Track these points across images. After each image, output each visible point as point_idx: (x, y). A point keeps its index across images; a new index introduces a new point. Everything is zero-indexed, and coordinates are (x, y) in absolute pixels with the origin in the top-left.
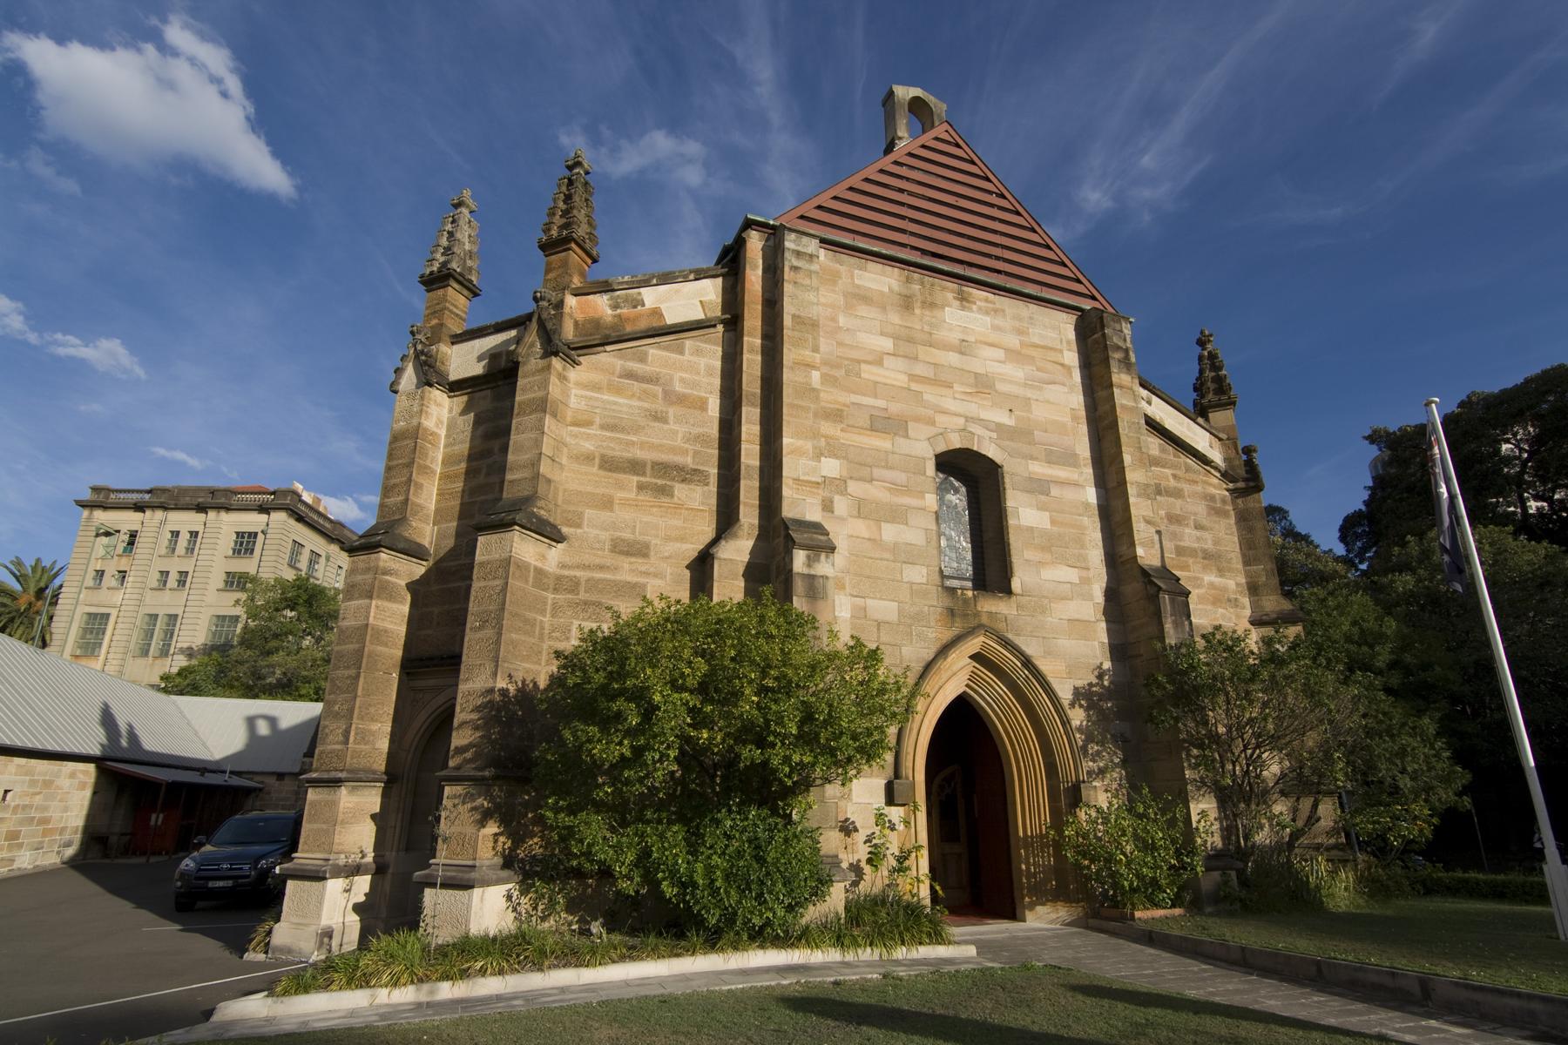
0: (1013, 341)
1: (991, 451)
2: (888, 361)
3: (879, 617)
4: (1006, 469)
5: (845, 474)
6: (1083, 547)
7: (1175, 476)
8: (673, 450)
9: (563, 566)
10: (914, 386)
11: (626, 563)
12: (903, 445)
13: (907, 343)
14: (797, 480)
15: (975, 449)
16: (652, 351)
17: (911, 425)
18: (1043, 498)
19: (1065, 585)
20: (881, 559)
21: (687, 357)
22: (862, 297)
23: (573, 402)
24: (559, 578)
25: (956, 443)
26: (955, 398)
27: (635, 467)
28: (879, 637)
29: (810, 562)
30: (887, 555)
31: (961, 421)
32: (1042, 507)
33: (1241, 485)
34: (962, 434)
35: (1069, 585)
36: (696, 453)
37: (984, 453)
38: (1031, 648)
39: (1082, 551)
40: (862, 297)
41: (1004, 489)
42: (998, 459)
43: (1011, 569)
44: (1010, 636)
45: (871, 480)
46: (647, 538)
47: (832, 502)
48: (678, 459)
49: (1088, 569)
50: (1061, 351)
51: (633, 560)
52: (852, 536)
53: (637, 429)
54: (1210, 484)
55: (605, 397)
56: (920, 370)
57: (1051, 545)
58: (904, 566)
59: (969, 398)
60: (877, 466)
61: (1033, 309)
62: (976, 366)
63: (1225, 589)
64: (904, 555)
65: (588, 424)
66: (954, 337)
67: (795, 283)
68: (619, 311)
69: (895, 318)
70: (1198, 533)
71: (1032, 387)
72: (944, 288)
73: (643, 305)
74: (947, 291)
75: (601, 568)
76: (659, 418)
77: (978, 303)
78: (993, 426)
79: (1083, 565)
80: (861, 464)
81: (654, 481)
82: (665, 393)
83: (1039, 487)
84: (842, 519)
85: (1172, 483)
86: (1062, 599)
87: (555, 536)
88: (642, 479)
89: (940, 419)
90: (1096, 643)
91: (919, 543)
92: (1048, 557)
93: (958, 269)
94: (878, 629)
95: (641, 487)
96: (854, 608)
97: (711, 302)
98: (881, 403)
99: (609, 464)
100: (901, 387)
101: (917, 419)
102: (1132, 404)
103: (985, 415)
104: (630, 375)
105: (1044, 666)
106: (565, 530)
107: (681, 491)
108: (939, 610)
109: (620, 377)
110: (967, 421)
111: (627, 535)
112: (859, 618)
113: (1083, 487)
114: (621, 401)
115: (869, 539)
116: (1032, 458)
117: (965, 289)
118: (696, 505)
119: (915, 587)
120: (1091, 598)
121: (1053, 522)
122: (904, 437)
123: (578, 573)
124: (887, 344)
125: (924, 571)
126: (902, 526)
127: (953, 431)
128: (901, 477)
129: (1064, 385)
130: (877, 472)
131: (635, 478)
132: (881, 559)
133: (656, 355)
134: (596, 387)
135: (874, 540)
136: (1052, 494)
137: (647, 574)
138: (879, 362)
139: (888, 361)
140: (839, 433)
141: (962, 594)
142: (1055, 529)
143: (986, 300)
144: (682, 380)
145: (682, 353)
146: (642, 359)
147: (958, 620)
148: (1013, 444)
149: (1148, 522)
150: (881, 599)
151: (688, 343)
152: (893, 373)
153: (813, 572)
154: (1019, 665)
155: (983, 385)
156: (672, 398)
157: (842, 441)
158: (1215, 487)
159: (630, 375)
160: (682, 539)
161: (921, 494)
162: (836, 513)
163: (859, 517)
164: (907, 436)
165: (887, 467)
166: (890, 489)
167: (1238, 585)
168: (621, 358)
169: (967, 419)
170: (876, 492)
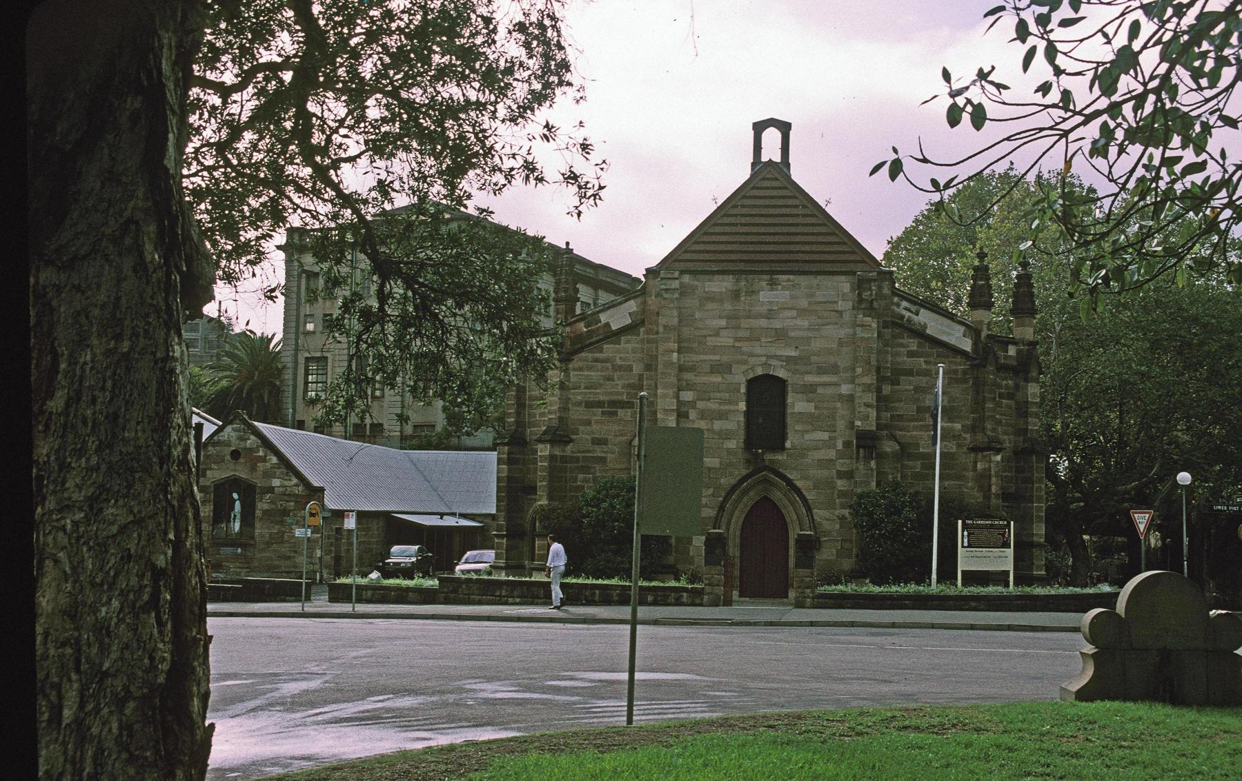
0: (804, 303)
1: (781, 374)
3: (709, 465)
4: (790, 382)
6: (834, 420)
8: (618, 394)
10: (737, 344)
11: (597, 448)
12: (729, 378)
13: (733, 317)
14: (665, 410)
16: (605, 346)
21: (622, 345)
23: (573, 379)
24: (572, 457)
25: (760, 371)
27: (600, 404)
31: (764, 359)
32: (808, 401)
36: (628, 393)
40: (710, 298)
42: (785, 378)
45: (709, 400)
48: (620, 398)
50: (837, 302)
53: (601, 385)
56: (741, 334)
57: (812, 421)
62: (777, 324)
63: (952, 429)
64: (725, 435)
65: (579, 388)
66: (764, 309)
69: (728, 306)
71: (817, 330)
72: (760, 280)
75: (589, 451)
76: (610, 379)
78: (784, 358)
82: (613, 366)
83: (810, 389)
85: (924, 366)
89: (753, 360)
95: (603, 413)
97: (634, 312)
98: (718, 357)
99: (589, 405)
101: (739, 362)
103: (779, 353)
104: (596, 360)
105: (799, 484)
107: (621, 412)
116: (808, 373)
120: (835, 446)
121: (816, 408)
124: (723, 323)
125: (735, 442)
129: (836, 324)
130: (712, 395)
133: (609, 349)
134: (580, 369)
136: (819, 391)
137: (605, 452)
138: (717, 335)
140: (693, 377)
143: (788, 280)
144: (621, 358)
145: (619, 343)
146: (601, 352)
149: (867, 405)
152: (726, 340)
155: (780, 335)
156: (617, 368)
159: (596, 360)
160: (622, 435)
163: (702, 419)
168: (591, 352)
170: (712, 405)
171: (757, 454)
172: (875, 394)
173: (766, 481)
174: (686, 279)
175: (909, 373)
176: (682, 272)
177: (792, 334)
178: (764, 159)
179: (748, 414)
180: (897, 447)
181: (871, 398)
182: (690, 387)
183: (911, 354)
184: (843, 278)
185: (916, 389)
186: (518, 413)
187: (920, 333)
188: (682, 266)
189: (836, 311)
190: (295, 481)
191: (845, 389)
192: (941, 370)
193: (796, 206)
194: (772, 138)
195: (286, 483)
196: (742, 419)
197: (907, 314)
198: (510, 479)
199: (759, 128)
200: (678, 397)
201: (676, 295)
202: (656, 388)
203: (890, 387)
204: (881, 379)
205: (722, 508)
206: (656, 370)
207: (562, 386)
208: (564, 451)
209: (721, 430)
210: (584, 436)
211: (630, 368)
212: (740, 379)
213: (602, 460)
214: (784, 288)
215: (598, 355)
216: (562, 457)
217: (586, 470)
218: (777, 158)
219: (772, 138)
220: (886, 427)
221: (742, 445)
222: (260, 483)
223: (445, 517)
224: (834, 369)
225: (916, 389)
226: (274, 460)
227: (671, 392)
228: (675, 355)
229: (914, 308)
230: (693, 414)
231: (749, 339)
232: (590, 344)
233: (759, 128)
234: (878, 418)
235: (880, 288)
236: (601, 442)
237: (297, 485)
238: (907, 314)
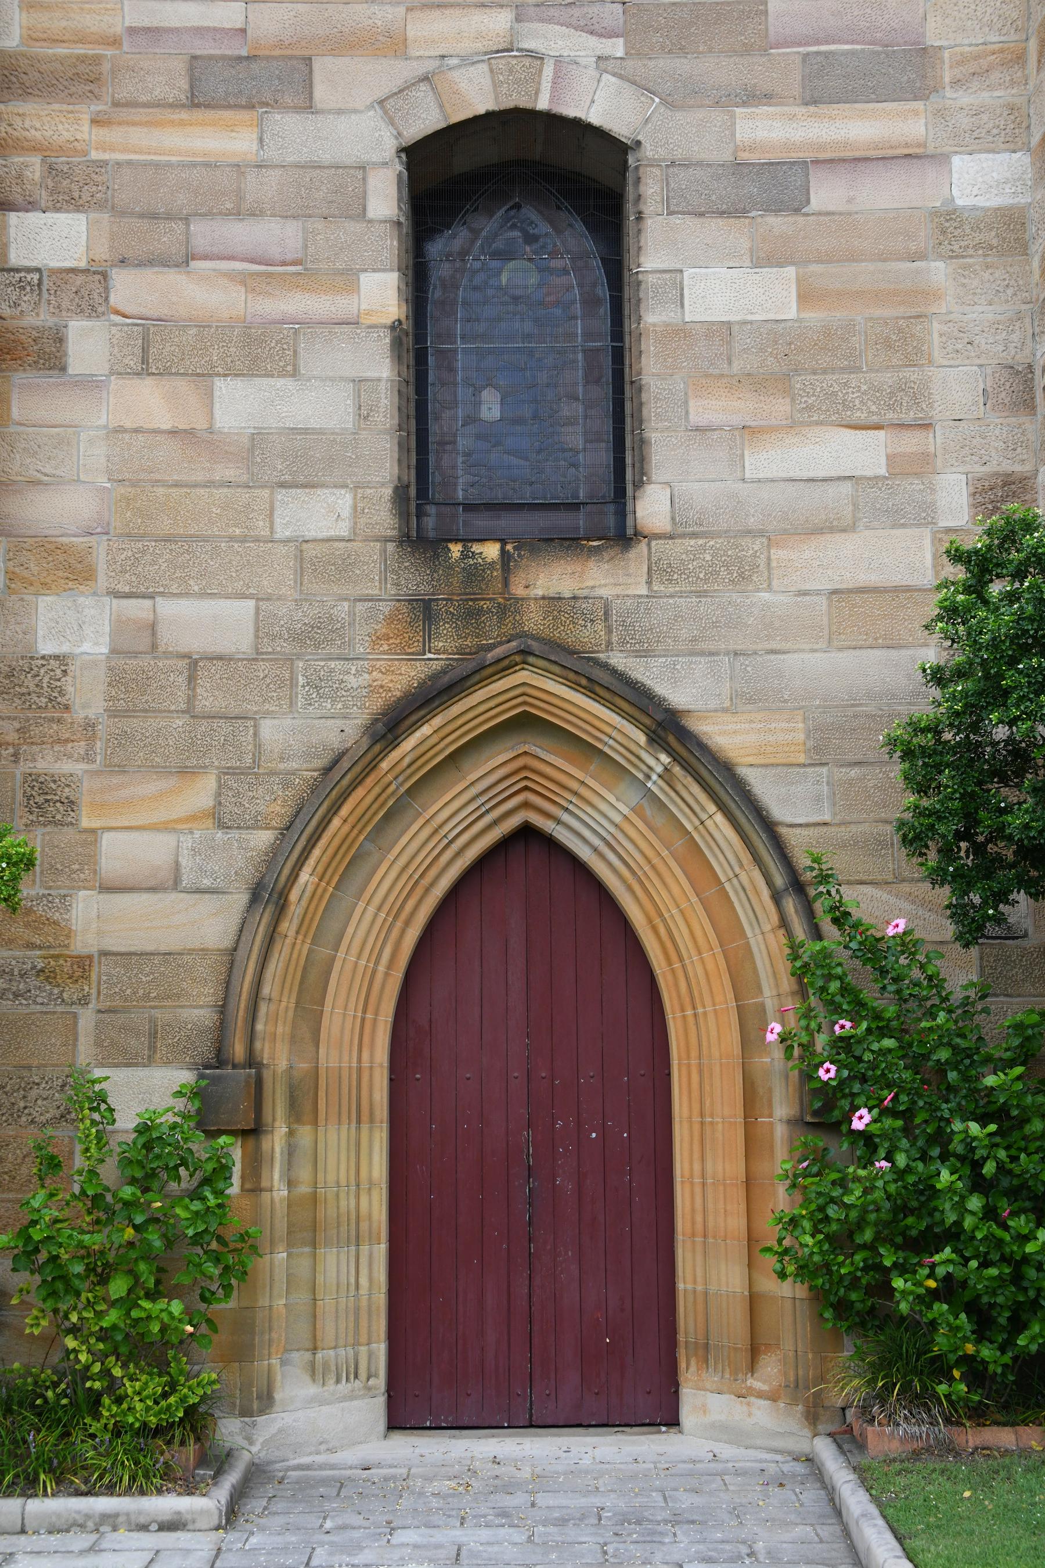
3: (195, 644)
4: (648, 151)
5: (102, 252)
15: (542, 104)
17: (317, 64)
18: (778, 223)
19: (832, 489)
20: (209, 484)
28: (191, 700)
30: (230, 472)
35: (847, 488)
37: (571, 111)
39: (912, 375)
42: (620, 128)
43: (642, 461)
44: (618, 660)
45: (187, 259)
47: (60, 340)
52: (120, 430)
58: (281, 495)
60: (209, 214)
79: (909, 417)
80: (154, 216)
84: (90, 384)
91: (333, 424)
92: (779, 408)
94: (192, 679)
96: (119, 626)
108: (386, 608)
112: (135, 654)
113: (941, 159)
115: (173, 433)
116: (754, 97)
119: (310, 550)
121: (806, 297)
122: (297, 109)
125: (344, 501)
126: (280, 382)
127: (467, 61)
132: (209, 484)
135: (190, 433)
140: (84, 131)
141: (465, 555)
142: (814, 316)
147: (445, 628)
148: (683, 65)
150: (203, 595)
154: (642, 739)
157: (94, 155)
163: (145, 369)
164: (308, 106)
165: (238, 213)
166: (243, 280)
171: (475, 574)
209: (258, 438)
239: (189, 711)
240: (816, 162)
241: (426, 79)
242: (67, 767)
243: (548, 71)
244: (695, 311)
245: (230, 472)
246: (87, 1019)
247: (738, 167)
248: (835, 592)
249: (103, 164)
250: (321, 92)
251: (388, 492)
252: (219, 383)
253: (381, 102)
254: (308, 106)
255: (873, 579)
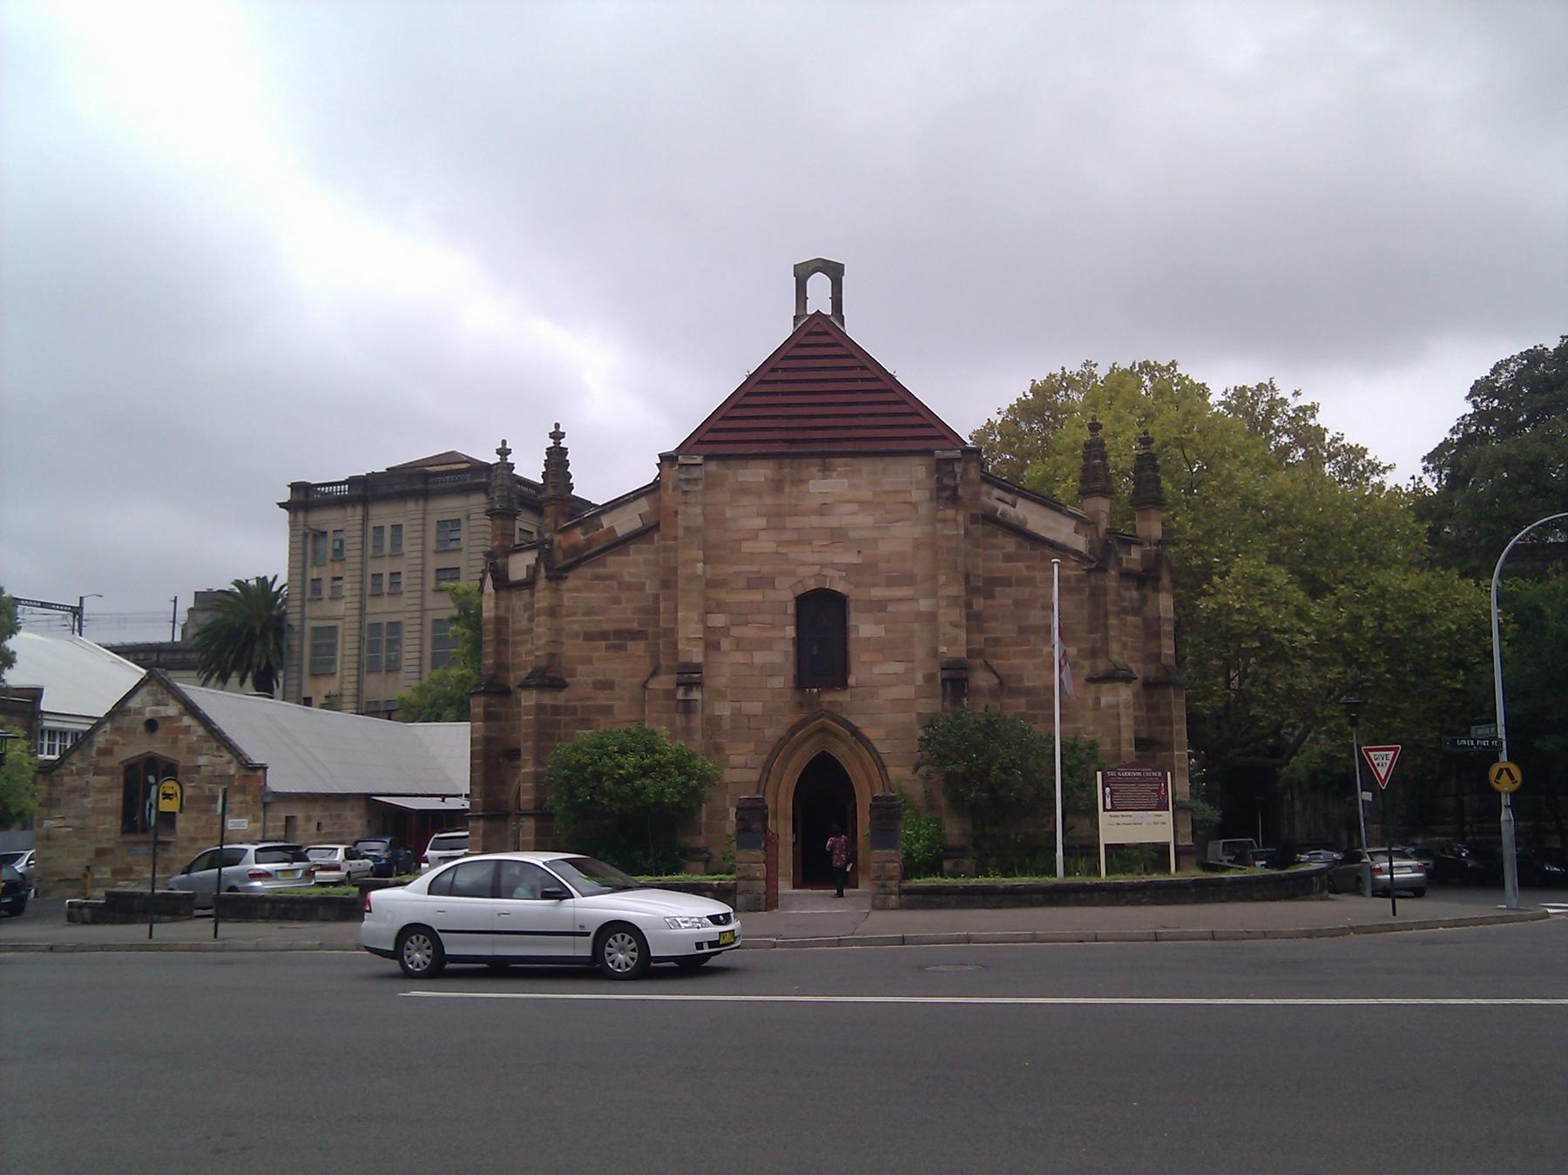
0: (867, 494)
1: (840, 587)
2: (762, 535)
4: (851, 597)
7: (1028, 568)
9: (568, 700)
10: (781, 550)
11: (601, 694)
12: (771, 595)
13: (776, 518)
14: (689, 640)
15: (827, 587)
22: (744, 491)
23: (567, 603)
25: (812, 585)
26: (813, 552)
27: (603, 635)
29: (686, 693)
32: (877, 623)
33: (1093, 566)
34: (818, 578)
38: (857, 721)
40: (744, 491)
41: (849, 613)
43: (849, 669)
44: (844, 716)
45: (747, 624)
46: (613, 678)
47: (719, 643)
49: (913, 661)
50: (910, 492)
51: (606, 692)
54: (1067, 568)
55: (584, 595)
56: (786, 536)
57: (885, 649)
59: (823, 549)
61: (888, 461)
62: (832, 522)
65: (574, 614)
67: (686, 503)
68: (588, 536)
69: (769, 500)
70: (1044, 613)
73: (603, 527)
74: (812, 469)
75: (589, 699)
76: (616, 601)
77: (839, 469)
81: (614, 642)
85: (1025, 573)
86: (889, 686)
87: (558, 684)
88: (608, 642)
90: (914, 715)
93: (819, 448)
94: (749, 720)
95: (608, 648)
98: (756, 568)
99: (589, 637)
100: (773, 553)
102: (955, 532)
103: (837, 560)
105: (870, 733)
106: (567, 680)
107: (631, 645)
109: (591, 580)
110: (822, 567)
111: (601, 678)
113: (917, 600)
114: (593, 595)
117: (827, 460)
118: (641, 653)
121: (886, 630)
123: (578, 704)
124: (762, 522)
125: (782, 679)
128: (768, 618)
130: (750, 618)
131: (604, 643)
133: (614, 562)
134: (578, 590)
135: (749, 664)
136: (889, 609)
138: (754, 537)
139: (762, 535)
143: (846, 465)
145: (628, 555)
149: (955, 625)
151: (632, 547)
152: (766, 545)
153: (689, 698)
155: (838, 537)
156: (623, 586)
158: (1071, 569)
159: (597, 577)
161: (783, 628)
162: (722, 649)
164: (774, 588)
167: (1079, 650)
169: (823, 565)
170: (750, 632)
172: (964, 610)
173: (824, 729)
174: (713, 466)
175: (1006, 582)
176: (707, 458)
177: (852, 534)
178: (810, 311)
179: (799, 642)
180: (996, 681)
181: (957, 614)
182: (720, 607)
183: (1008, 558)
184: (917, 460)
185: (1018, 603)
186: (498, 653)
187: (1018, 531)
188: (709, 449)
189: (910, 503)
190: (227, 756)
191: (924, 605)
192: (1056, 567)
193: (853, 368)
194: (819, 287)
195: (218, 760)
196: (790, 648)
197: (1001, 507)
198: (488, 740)
199: (802, 273)
200: (703, 620)
201: (700, 487)
202: (676, 612)
203: (982, 600)
204: (971, 590)
205: (767, 768)
206: (676, 587)
207: (553, 612)
208: (556, 698)
210: (582, 678)
211: (641, 587)
212: (785, 594)
213: (608, 710)
214: (840, 475)
215: (600, 571)
216: (554, 707)
217: (586, 723)
218: (827, 310)
219: (819, 287)
220: (980, 653)
221: (791, 684)
222: (183, 760)
223: (447, 799)
224: (907, 579)
225: (1018, 603)
226: (201, 731)
227: (695, 615)
228: (700, 565)
229: (1009, 498)
230: (725, 644)
231: (797, 543)
232: (588, 557)
233: (802, 273)
234: (969, 642)
235: (965, 471)
236: (606, 685)
237: (229, 762)
238: (1001, 507)
239: (749, 728)
240: (890, 600)
241: (800, 581)
242: (722, 740)
243: (828, 579)
244: (861, 635)
245: (756, 673)
246: (728, 798)
247: (871, 601)
248: (893, 700)
249: (727, 603)
250: (777, 586)
251: (792, 677)
252: (755, 653)
253: (790, 587)
254: (774, 588)
255: (900, 697)
